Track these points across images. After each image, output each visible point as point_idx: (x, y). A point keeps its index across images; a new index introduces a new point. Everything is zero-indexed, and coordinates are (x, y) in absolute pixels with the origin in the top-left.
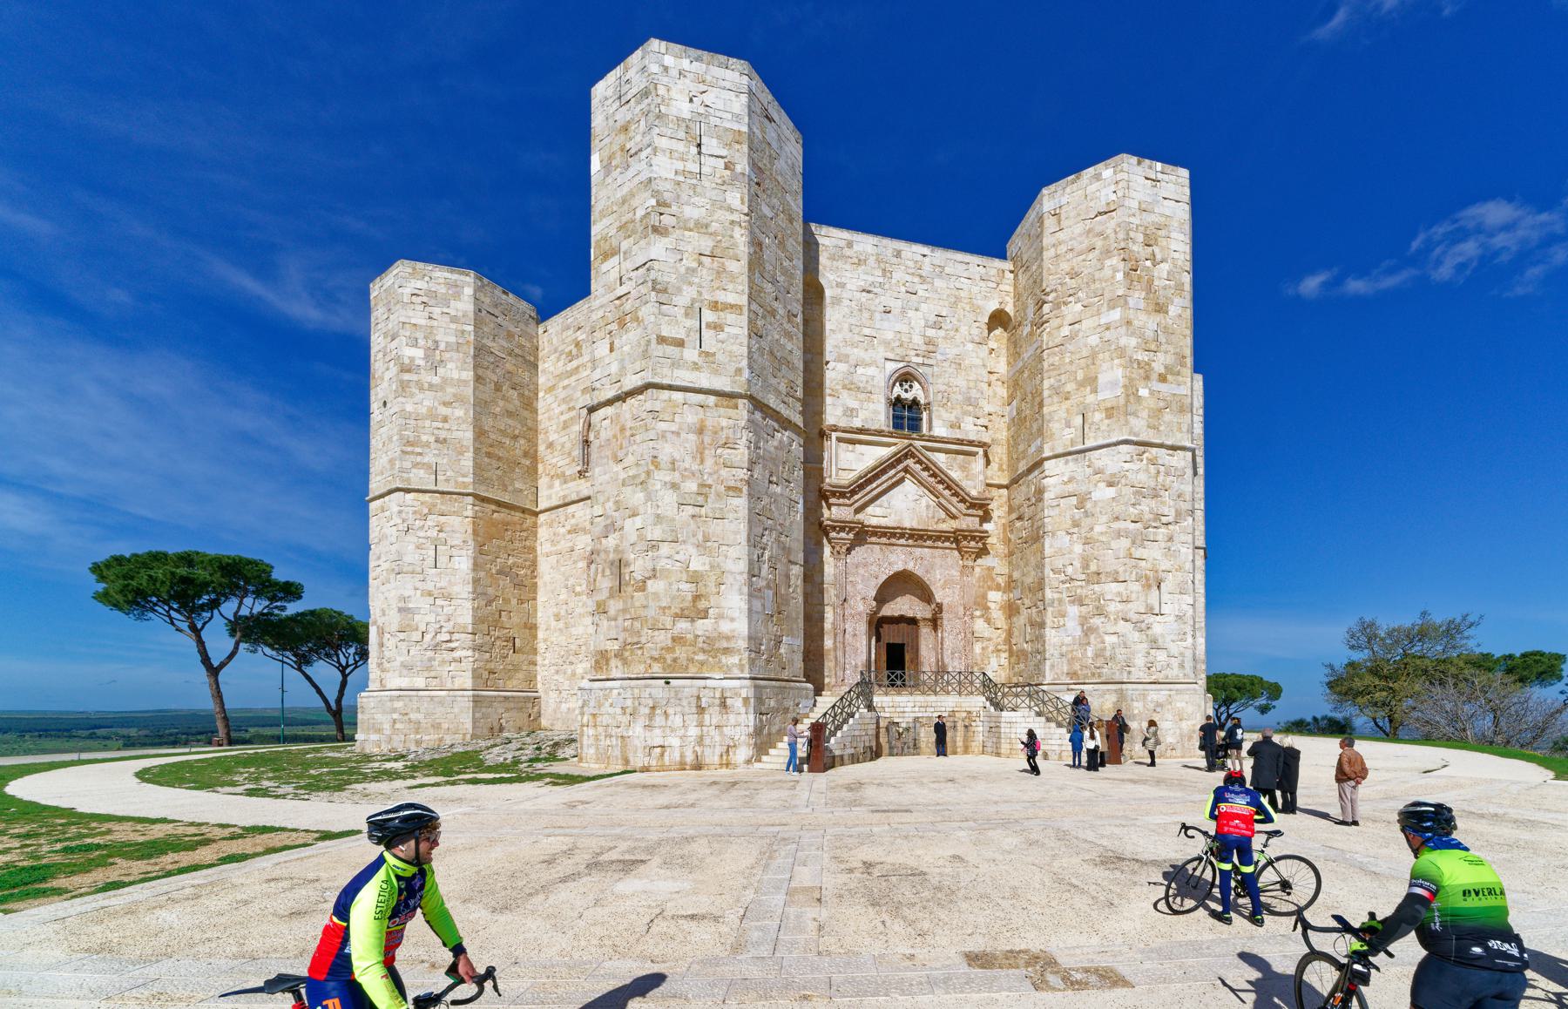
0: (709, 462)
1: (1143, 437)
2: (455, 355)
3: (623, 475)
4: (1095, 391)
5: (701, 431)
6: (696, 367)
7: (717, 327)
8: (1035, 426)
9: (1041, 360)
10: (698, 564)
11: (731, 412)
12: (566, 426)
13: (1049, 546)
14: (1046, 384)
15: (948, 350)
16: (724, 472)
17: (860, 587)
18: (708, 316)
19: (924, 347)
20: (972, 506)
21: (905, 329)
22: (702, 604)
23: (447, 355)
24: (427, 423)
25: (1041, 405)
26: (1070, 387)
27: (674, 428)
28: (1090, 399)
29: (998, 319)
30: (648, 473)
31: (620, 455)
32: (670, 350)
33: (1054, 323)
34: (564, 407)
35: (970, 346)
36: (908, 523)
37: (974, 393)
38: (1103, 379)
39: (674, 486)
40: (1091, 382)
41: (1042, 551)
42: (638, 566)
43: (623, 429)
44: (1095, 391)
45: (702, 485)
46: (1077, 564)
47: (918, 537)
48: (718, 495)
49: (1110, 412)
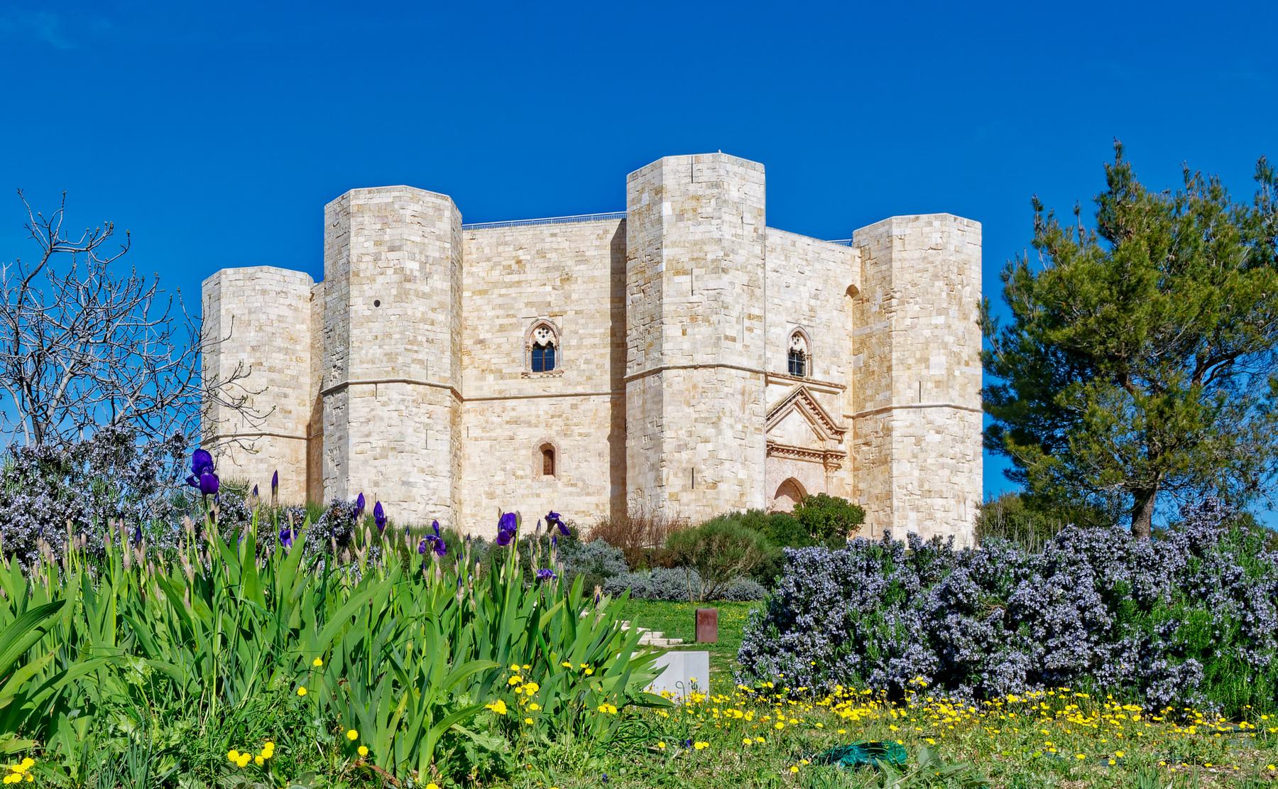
0: (747, 412)
2: (441, 269)
3: (695, 416)
4: (928, 367)
5: (743, 394)
6: (741, 355)
7: (750, 330)
8: (884, 382)
9: (890, 337)
10: (742, 474)
11: (757, 382)
12: (502, 328)
13: (896, 469)
14: (894, 355)
15: (823, 316)
18: (747, 323)
20: (836, 432)
21: (797, 299)
22: (744, 499)
23: (433, 268)
24: (421, 325)
25: (890, 368)
26: (911, 361)
28: (924, 372)
29: (852, 291)
30: (719, 418)
31: (693, 402)
32: (730, 343)
33: (901, 314)
34: (501, 312)
35: (835, 312)
37: (837, 349)
38: (933, 360)
39: (732, 427)
40: (925, 360)
41: (890, 472)
42: (708, 474)
43: (695, 387)
44: (928, 367)
46: (916, 484)
49: (938, 384)
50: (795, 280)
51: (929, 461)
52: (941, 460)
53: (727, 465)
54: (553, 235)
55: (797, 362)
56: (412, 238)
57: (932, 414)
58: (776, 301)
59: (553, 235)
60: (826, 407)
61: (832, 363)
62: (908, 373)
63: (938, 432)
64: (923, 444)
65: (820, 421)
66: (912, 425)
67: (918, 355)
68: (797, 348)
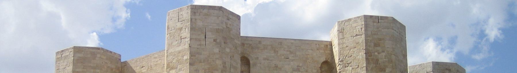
54: (156, 58)
56: (77, 70)
59: (156, 58)
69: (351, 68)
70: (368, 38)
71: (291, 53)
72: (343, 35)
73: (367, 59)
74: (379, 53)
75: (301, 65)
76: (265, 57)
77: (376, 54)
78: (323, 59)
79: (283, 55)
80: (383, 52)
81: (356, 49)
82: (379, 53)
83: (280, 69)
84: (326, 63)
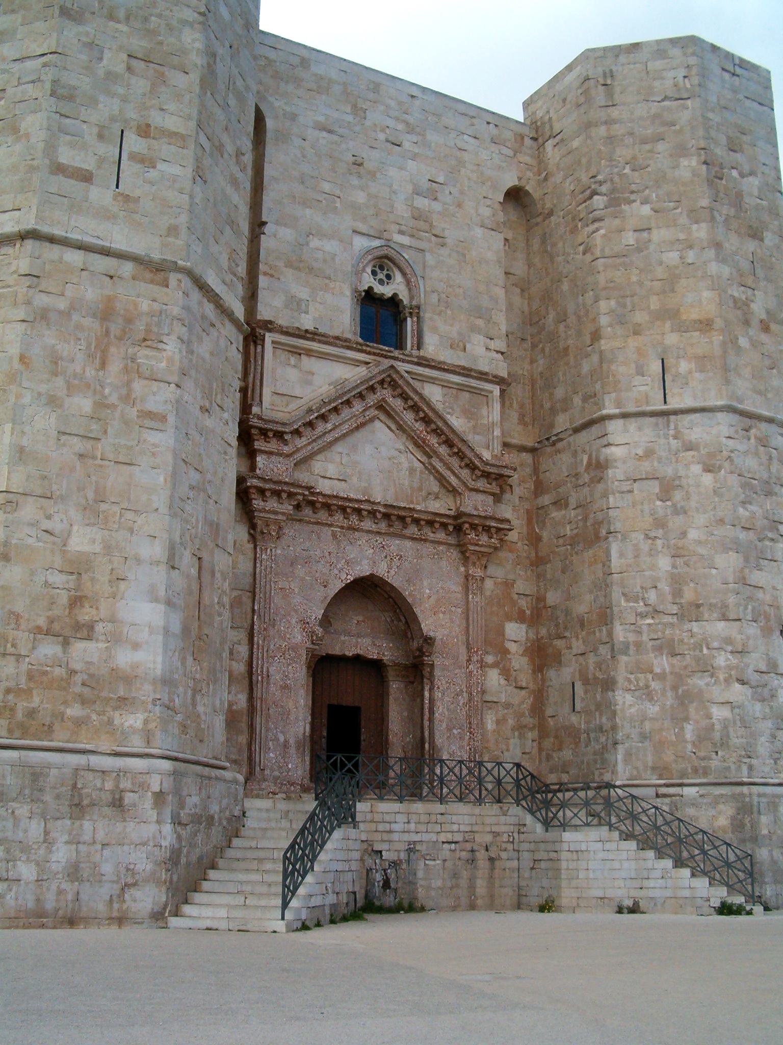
0: (115, 366)
1: (747, 406)
16: (138, 386)
17: (297, 600)
19: (412, 223)
25: (596, 336)
26: (640, 317)
27: (62, 305)
35: (479, 232)
36: (378, 496)
39: (53, 402)
45: (101, 405)
47: (396, 519)
48: (126, 422)
50: (375, 154)
51: (693, 534)
52: (720, 532)
53: (29, 510)
55: (383, 319)
57: (698, 430)
58: (326, 187)
60: (457, 422)
61: (474, 329)
62: (633, 343)
63: (708, 469)
64: (678, 496)
65: (443, 450)
66: (649, 453)
67: (654, 303)
68: (387, 291)
69: (646, 210)
70: (710, 115)
71: (411, 129)
72: (610, 94)
73: (710, 183)
74: (742, 175)
75: (441, 179)
76: (321, 119)
77: (735, 173)
78: (510, 180)
79: (383, 130)
80: (752, 173)
81: (660, 147)
82: (742, 175)
83: (372, 175)
84: (515, 195)
